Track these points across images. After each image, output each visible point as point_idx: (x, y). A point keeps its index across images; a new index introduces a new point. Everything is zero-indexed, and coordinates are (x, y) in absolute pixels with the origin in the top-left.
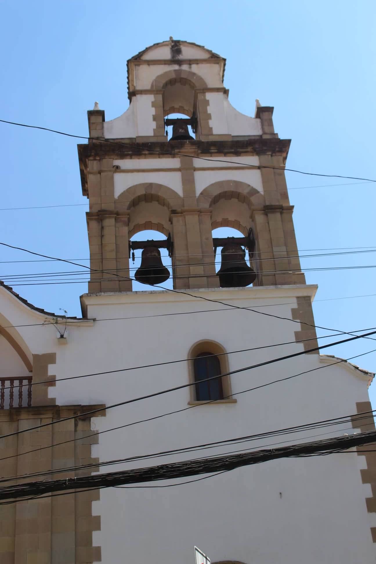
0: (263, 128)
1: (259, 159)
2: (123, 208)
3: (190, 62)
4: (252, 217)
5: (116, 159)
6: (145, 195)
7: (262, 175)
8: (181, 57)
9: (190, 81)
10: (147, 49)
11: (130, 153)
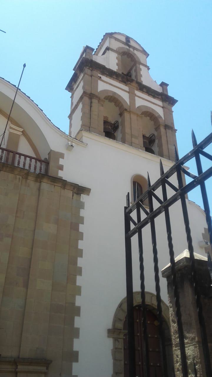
0: (163, 91)
1: (163, 104)
2: (102, 97)
3: (134, 48)
4: (157, 128)
5: (99, 74)
6: (112, 96)
7: (164, 111)
8: (130, 44)
9: (133, 56)
10: (115, 33)
11: (107, 73)
